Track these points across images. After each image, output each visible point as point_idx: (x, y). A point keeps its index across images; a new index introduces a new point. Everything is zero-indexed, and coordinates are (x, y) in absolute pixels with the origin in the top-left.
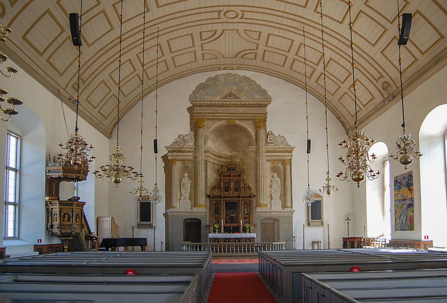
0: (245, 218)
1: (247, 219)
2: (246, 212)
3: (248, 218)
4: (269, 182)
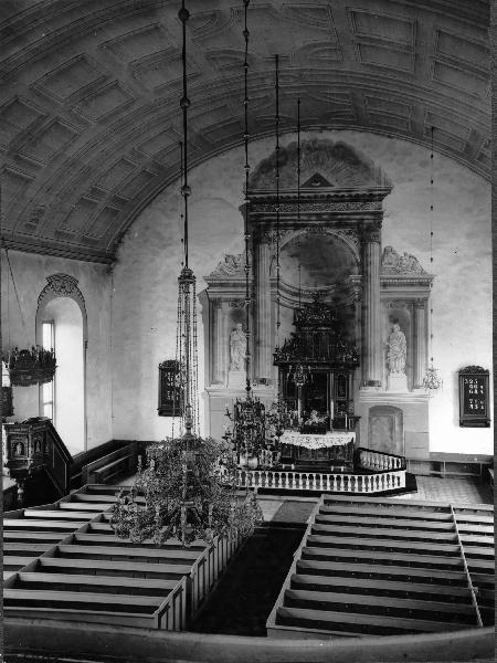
4: (384, 339)
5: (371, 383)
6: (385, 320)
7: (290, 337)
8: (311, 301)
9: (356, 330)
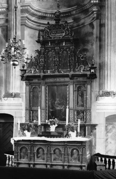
0: (78, 113)
1: (82, 114)
2: (80, 103)
5: (108, 94)
7: (34, 55)
8: (53, 22)
9: (94, 46)
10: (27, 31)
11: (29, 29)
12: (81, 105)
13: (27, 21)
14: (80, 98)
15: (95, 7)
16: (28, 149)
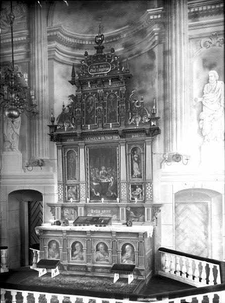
0: (134, 187)
2: (137, 172)
3: (141, 187)
5: (177, 158)
6: (196, 65)
8: (92, 53)
9: (156, 86)
10: (58, 69)
11: (59, 65)
12: (138, 175)
13: (56, 53)
14: (136, 165)
15: (156, 26)
16: (59, 243)
